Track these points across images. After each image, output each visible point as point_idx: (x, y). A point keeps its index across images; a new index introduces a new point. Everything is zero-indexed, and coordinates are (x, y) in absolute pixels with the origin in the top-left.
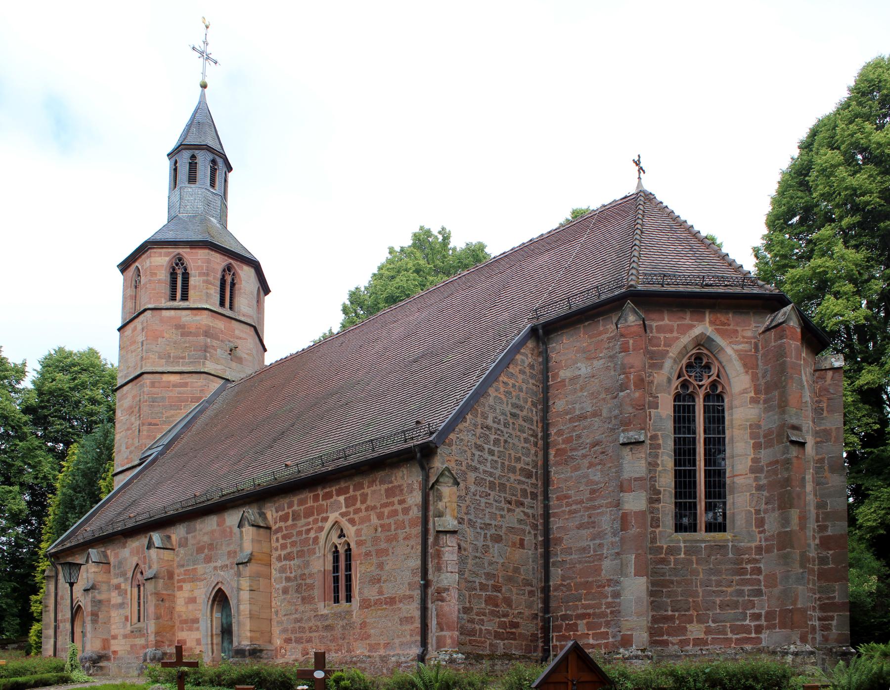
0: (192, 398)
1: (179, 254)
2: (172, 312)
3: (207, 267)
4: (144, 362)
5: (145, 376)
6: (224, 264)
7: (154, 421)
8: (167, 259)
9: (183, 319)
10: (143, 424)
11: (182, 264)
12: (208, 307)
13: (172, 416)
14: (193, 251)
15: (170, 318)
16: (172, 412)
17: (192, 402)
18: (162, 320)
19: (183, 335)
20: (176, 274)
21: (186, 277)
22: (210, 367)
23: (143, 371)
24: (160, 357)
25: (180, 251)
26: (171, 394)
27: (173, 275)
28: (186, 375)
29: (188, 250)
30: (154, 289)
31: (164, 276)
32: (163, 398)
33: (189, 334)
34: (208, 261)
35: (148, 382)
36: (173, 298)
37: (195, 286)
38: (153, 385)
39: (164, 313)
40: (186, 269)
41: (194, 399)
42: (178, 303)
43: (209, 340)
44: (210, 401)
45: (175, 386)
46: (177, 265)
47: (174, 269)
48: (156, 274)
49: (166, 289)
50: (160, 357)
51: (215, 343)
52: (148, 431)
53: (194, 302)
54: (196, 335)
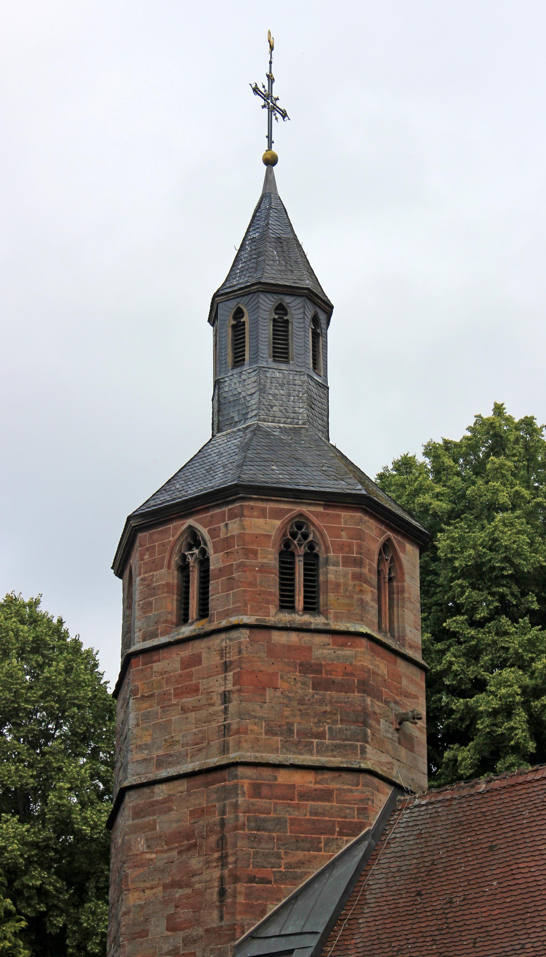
0: (343, 825)
1: (301, 515)
2: (294, 637)
3: (360, 546)
4: (231, 740)
5: (241, 770)
6: (381, 540)
7: (260, 873)
8: (278, 523)
9: (317, 653)
10: (236, 879)
11: (305, 536)
12: (364, 629)
13: (301, 863)
14: (330, 512)
15: (290, 648)
16: (301, 855)
17: (341, 833)
18: (272, 651)
19: (316, 686)
20: (292, 555)
21: (312, 562)
22: (373, 759)
23: (233, 756)
24: (270, 732)
25: (304, 509)
26: (296, 814)
27: (286, 557)
28: (328, 775)
29: (321, 509)
30: (252, 584)
31: (270, 557)
32: (280, 822)
33: (330, 685)
34: (359, 535)
35: (246, 784)
36: (287, 604)
37: (338, 585)
38: (256, 790)
39: (278, 637)
40: (311, 546)
42: (302, 619)
43: (369, 700)
44: (378, 834)
45: (305, 796)
46: (294, 535)
47: (287, 544)
48: (255, 553)
49: (272, 584)
50: (270, 732)
51: (377, 706)
52: (248, 895)
53: (337, 618)
54: (346, 687)
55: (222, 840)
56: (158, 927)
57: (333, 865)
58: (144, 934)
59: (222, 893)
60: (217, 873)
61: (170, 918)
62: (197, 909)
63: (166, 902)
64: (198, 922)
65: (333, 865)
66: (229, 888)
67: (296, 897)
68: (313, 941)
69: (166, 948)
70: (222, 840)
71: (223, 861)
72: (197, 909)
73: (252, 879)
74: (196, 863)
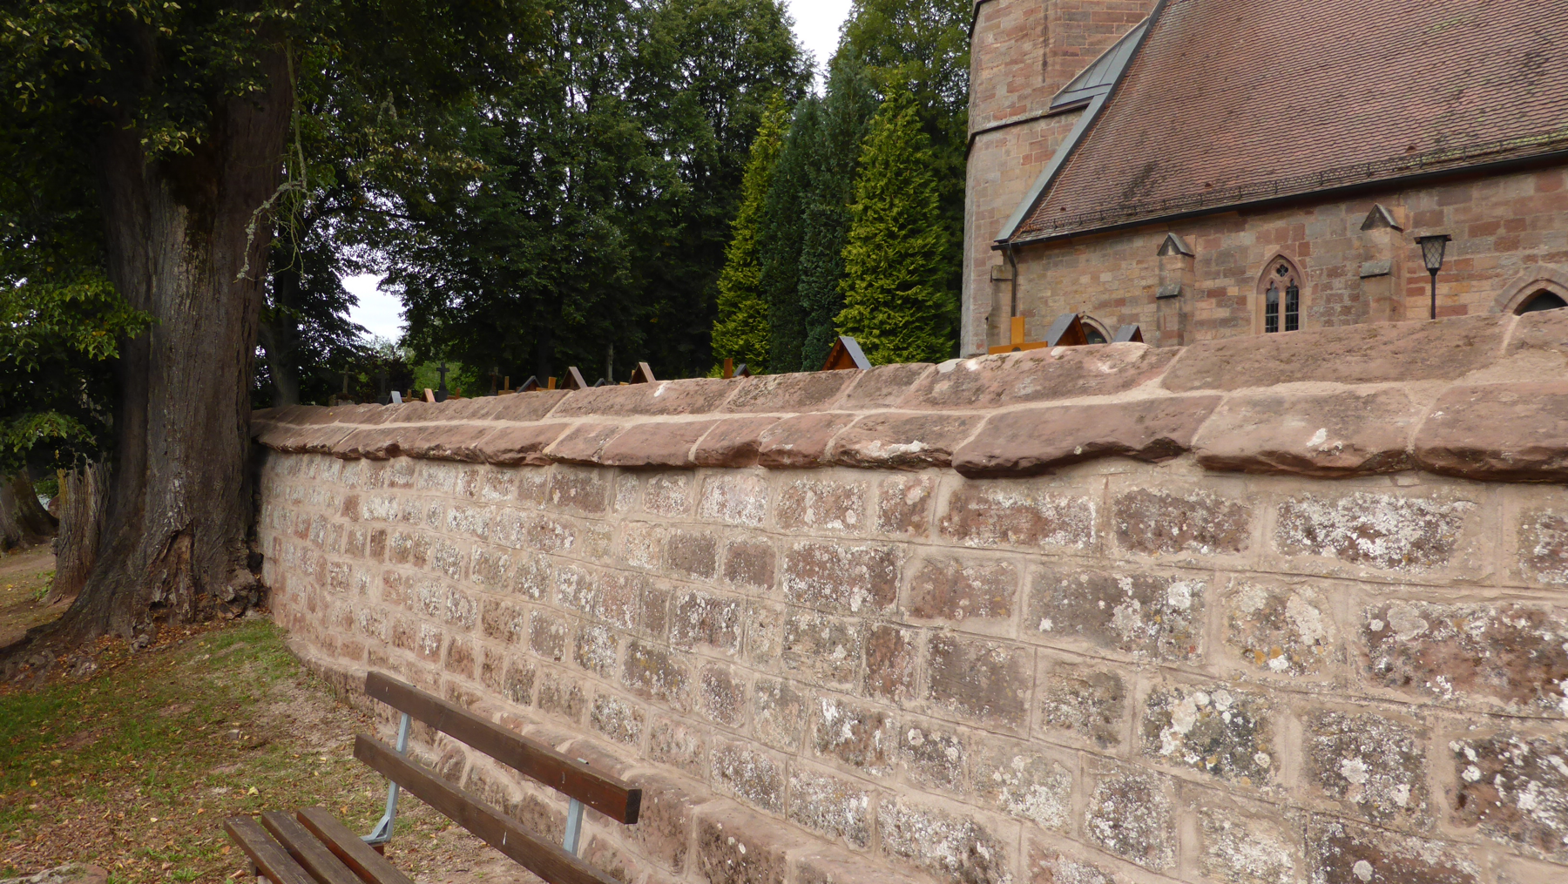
13: (1099, 42)
16: (1099, 36)
41: (1134, 18)
44: (1154, 22)
55: (1046, 28)
56: (1002, 91)
57: (1122, 42)
58: (993, 96)
59: (1045, 64)
60: (1041, 52)
61: (1010, 84)
62: (1027, 77)
63: (1006, 75)
64: (1028, 85)
65: (1122, 42)
66: (1050, 60)
67: (1095, 65)
68: (1108, 89)
69: (1007, 103)
70: (1046, 28)
71: (1046, 42)
72: (1027, 77)
73: (1066, 54)
74: (1027, 46)
